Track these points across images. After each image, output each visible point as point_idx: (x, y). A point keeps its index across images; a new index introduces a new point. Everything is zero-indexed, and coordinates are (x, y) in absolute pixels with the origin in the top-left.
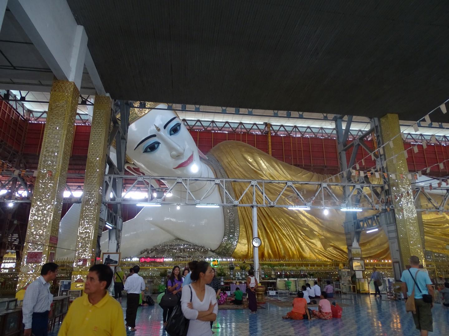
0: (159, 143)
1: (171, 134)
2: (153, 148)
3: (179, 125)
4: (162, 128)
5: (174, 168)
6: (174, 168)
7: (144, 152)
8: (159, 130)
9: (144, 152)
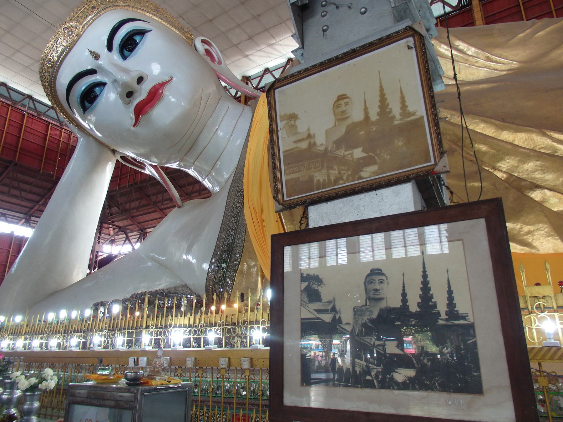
0: (103, 84)
1: (124, 58)
2: (89, 98)
3: (142, 33)
4: (103, 51)
5: (134, 126)
6: (134, 126)
7: (84, 113)
8: (96, 57)
9: (84, 113)
